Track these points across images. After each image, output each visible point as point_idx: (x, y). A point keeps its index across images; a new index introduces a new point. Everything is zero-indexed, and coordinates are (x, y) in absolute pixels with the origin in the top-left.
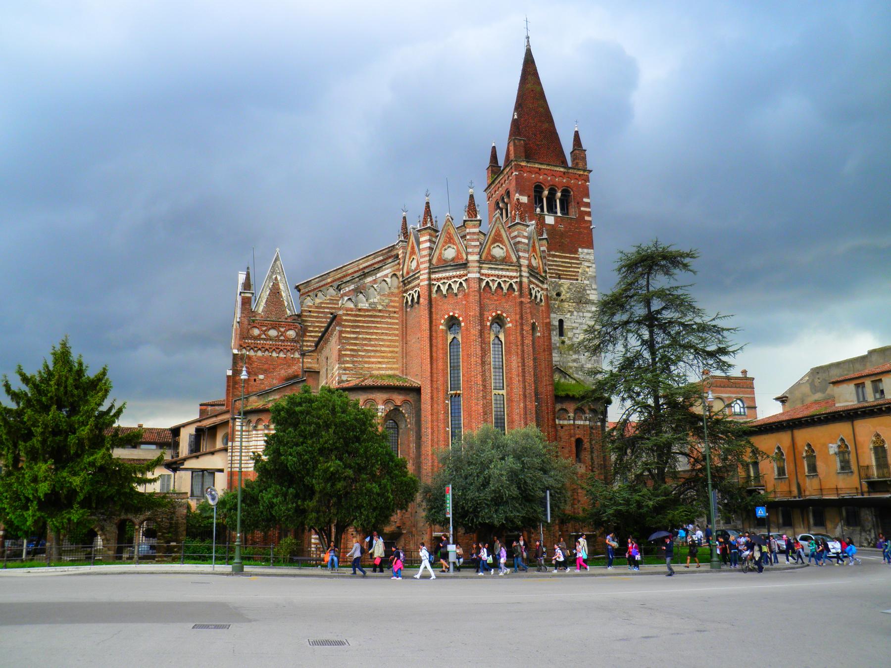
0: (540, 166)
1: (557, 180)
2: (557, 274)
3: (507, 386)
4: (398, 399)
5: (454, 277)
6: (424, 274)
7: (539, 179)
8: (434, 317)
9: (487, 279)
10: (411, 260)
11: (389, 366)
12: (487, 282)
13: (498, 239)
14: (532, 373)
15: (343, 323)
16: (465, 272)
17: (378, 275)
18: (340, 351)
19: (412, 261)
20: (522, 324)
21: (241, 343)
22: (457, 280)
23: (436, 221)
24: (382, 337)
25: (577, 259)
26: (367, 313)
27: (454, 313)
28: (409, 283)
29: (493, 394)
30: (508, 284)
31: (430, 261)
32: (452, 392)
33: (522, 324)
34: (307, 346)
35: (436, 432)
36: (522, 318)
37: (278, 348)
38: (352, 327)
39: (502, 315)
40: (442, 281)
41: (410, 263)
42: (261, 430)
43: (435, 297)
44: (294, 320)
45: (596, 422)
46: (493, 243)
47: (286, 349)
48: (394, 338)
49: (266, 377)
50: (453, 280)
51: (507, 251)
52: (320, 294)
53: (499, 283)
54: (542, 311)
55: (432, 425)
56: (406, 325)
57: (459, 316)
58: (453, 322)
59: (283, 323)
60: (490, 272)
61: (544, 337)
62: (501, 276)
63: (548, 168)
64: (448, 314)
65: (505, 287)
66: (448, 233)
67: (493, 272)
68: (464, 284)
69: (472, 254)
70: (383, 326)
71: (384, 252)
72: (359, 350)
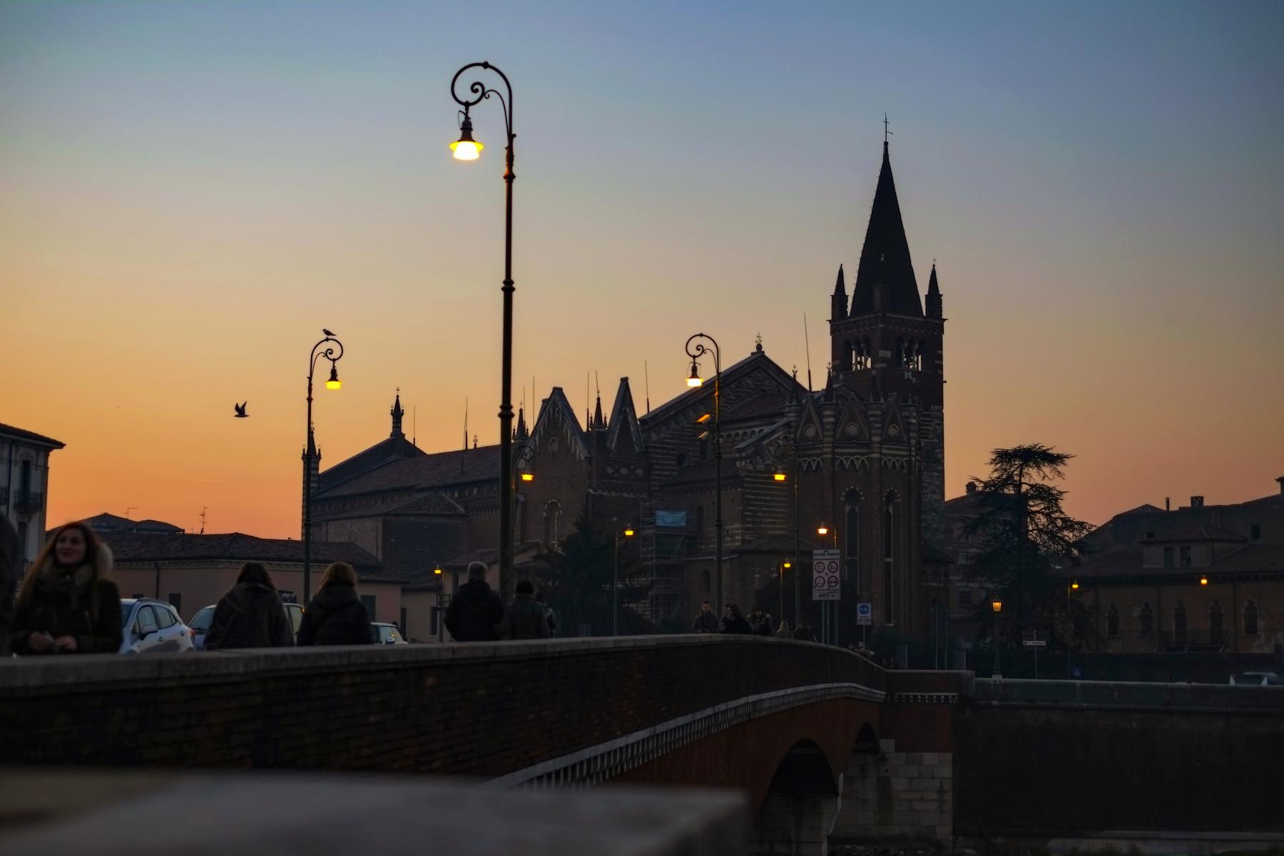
0: (903, 317)
6: (828, 447)
9: (885, 459)
15: (746, 485)
16: (868, 451)
17: (773, 438)
25: (929, 416)
26: (763, 475)
30: (900, 462)
31: (834, 436)
32: (849, 558)
39: (894, 490)
40: (845, 457)
51: (900, 429)
64: (849, 488)
69: (875, 435)
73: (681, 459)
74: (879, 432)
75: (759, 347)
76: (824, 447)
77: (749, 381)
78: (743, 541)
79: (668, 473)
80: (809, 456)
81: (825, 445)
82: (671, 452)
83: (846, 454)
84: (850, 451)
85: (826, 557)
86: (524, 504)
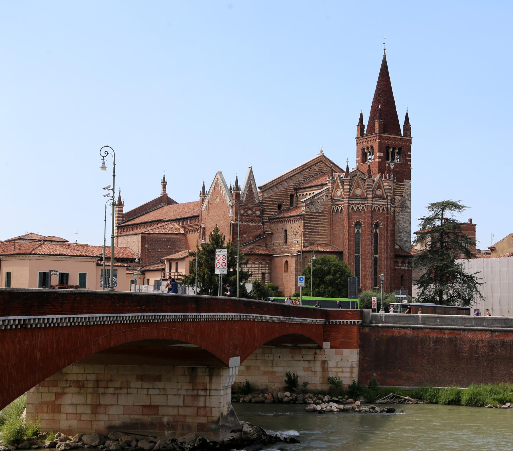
0: (390, 136)
3: (379, 253)
5: (360, 204)
7: (389, 143)
9: (374, 206)
11: (323, 239)
13: (379, 187)
16: (365, 202)
17: (320, 196)
18: (304, 232)
20: (387, 227)
22: (361, 205)
25: (403, 185)
27: (359, 220)
28: (336, 202)
31: (349, 195)
33: (387, 227)
36: (387, 224)
38: (309, 220)
40: (354, 205)
42: (250, 264)
43: (351, 212)
45: (409, 268)
46: (377, 189)
50: (359, 205)
51: (383, 192)
52: (270, 191)
53: (379, 208)
57: (361, 222)
58: (358, 224)
59: (254, 207)
63: (393, 136)
64: (356, 220)
65: (381, 209)
66: (358, 182)
67: (377, 203)
69: (369, 194)
70: (321, 220)
73: (279, 207)
74: (371, 193)
75: (322, 151)
76: (344, 200)
77: (316, 168)
78: (304, 247)
79: (273, 213)
80: (337, 205)
81: (345, 199)
83: (355, 204)
85: (221, 253)
86: (204, 228)
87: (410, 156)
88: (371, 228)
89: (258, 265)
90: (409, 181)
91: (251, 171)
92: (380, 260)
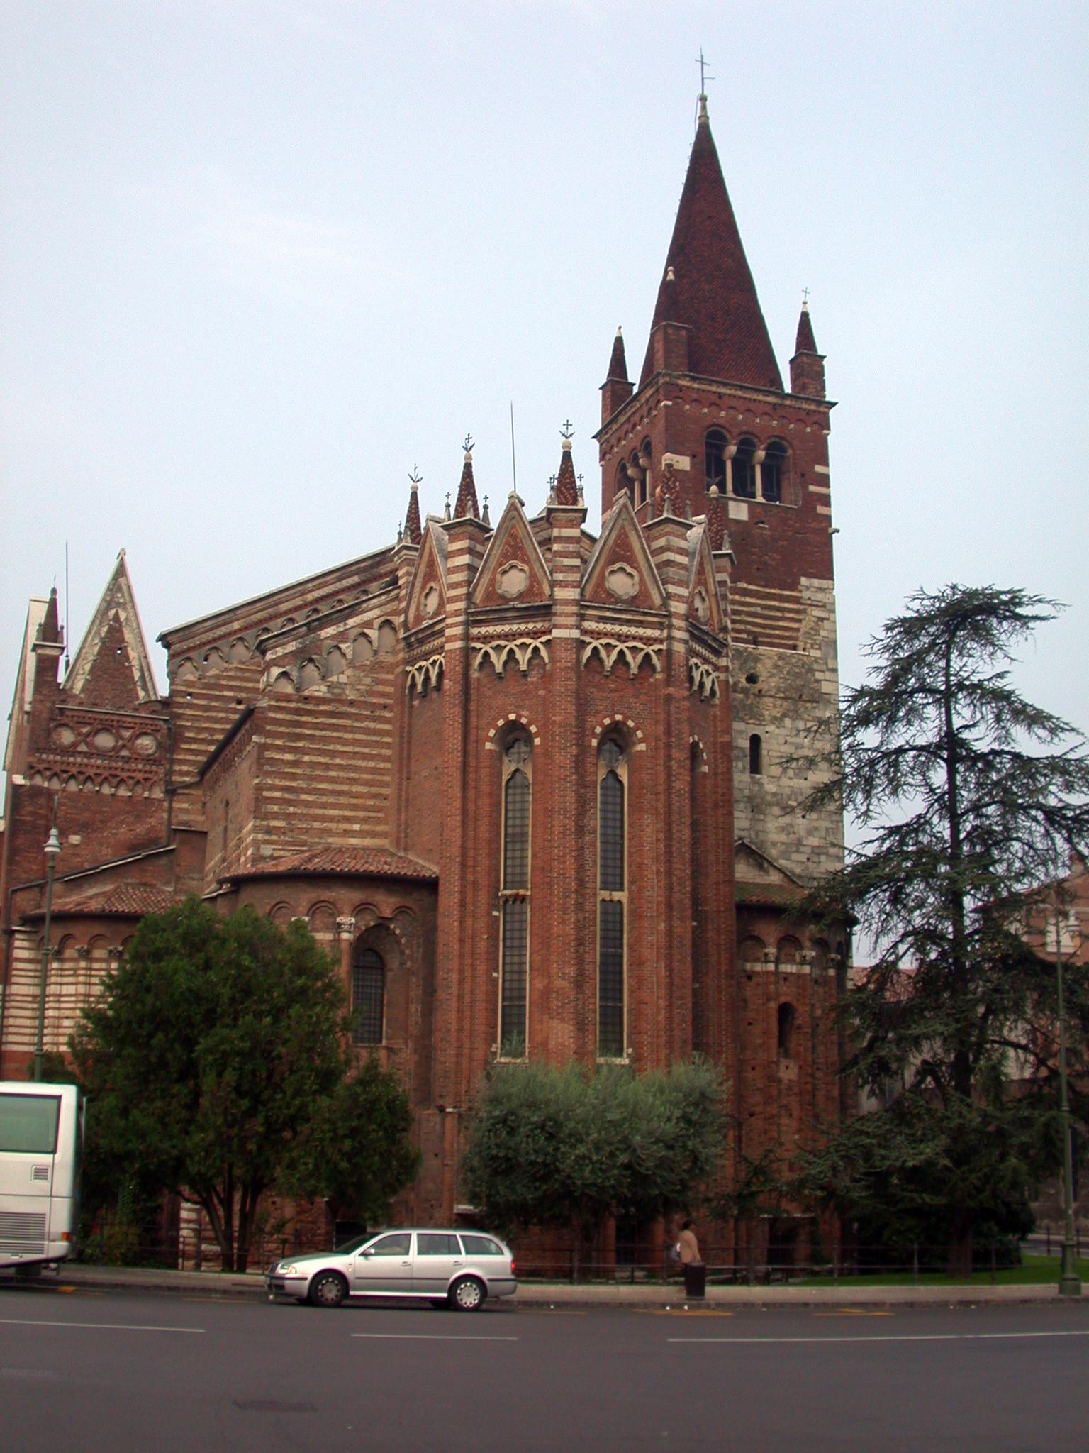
1: (758, 421)
2: (749, 632)
3: (631, 883)
4: (386, 903)
5: (521, 635)
6: (455, 625)
7: (718, 417)
8: (473, 720)
9: (595, 643)
10: (427, 591)
11: (366, 827)
12: (595, 650)
14: (688, 856)
15: (268, 728)
16: (547, 625)
17: (351, 622)
18: (259, 788)
19: (427, 594)
20: (668, 746)
21: (31, 759)
22: (528, 641)
23: (486, 507)
24: (354, 762)
25: (797, 600)
27: (519, 716)
28: (421, 642)
29: (599, 899)
30: (640, 656)
31: (469, 597)
32: (508, 892)
33: (668, 746)
34: (182, 774)
35: (468, 980)
36: (668, 733)
37: (115, 776)
39: (624, 723)
40: (494, 644)
41: (423, 598)
43: (478, 679)
44: (154, 712)
45: (826, 969)
47: (133, 778)
48: (382, 765)
49: (87, 841)
50: (519, 642)
51: (642, 581)
53: (621, 653)
54: (715, 717)
55: (460, 964)
56: (410, 738)
57: (530, 724)
58: (513, 735)
59: (128, 719)
60: (601, 626)
61: (716, 774)
62: (627, 637)
64: (506, 718)
65: (634, 662)
66: (511, 535)
68: (544, 652)
69: (564, 584)
71: (363, 565)
72: (302, 791)
80: (426, 656)
82: (233, 705)
83: (499, 637)
84: (507, 628)
87: (824, 480)
88: (574, 750)
89: (104, 966)
90: (824, 583)
91: (121, 571)
92: (637, 916)
